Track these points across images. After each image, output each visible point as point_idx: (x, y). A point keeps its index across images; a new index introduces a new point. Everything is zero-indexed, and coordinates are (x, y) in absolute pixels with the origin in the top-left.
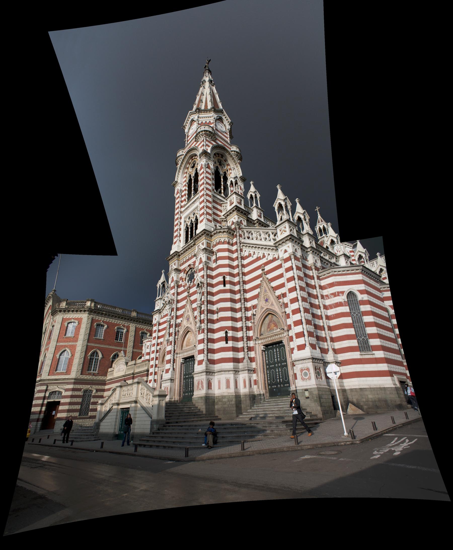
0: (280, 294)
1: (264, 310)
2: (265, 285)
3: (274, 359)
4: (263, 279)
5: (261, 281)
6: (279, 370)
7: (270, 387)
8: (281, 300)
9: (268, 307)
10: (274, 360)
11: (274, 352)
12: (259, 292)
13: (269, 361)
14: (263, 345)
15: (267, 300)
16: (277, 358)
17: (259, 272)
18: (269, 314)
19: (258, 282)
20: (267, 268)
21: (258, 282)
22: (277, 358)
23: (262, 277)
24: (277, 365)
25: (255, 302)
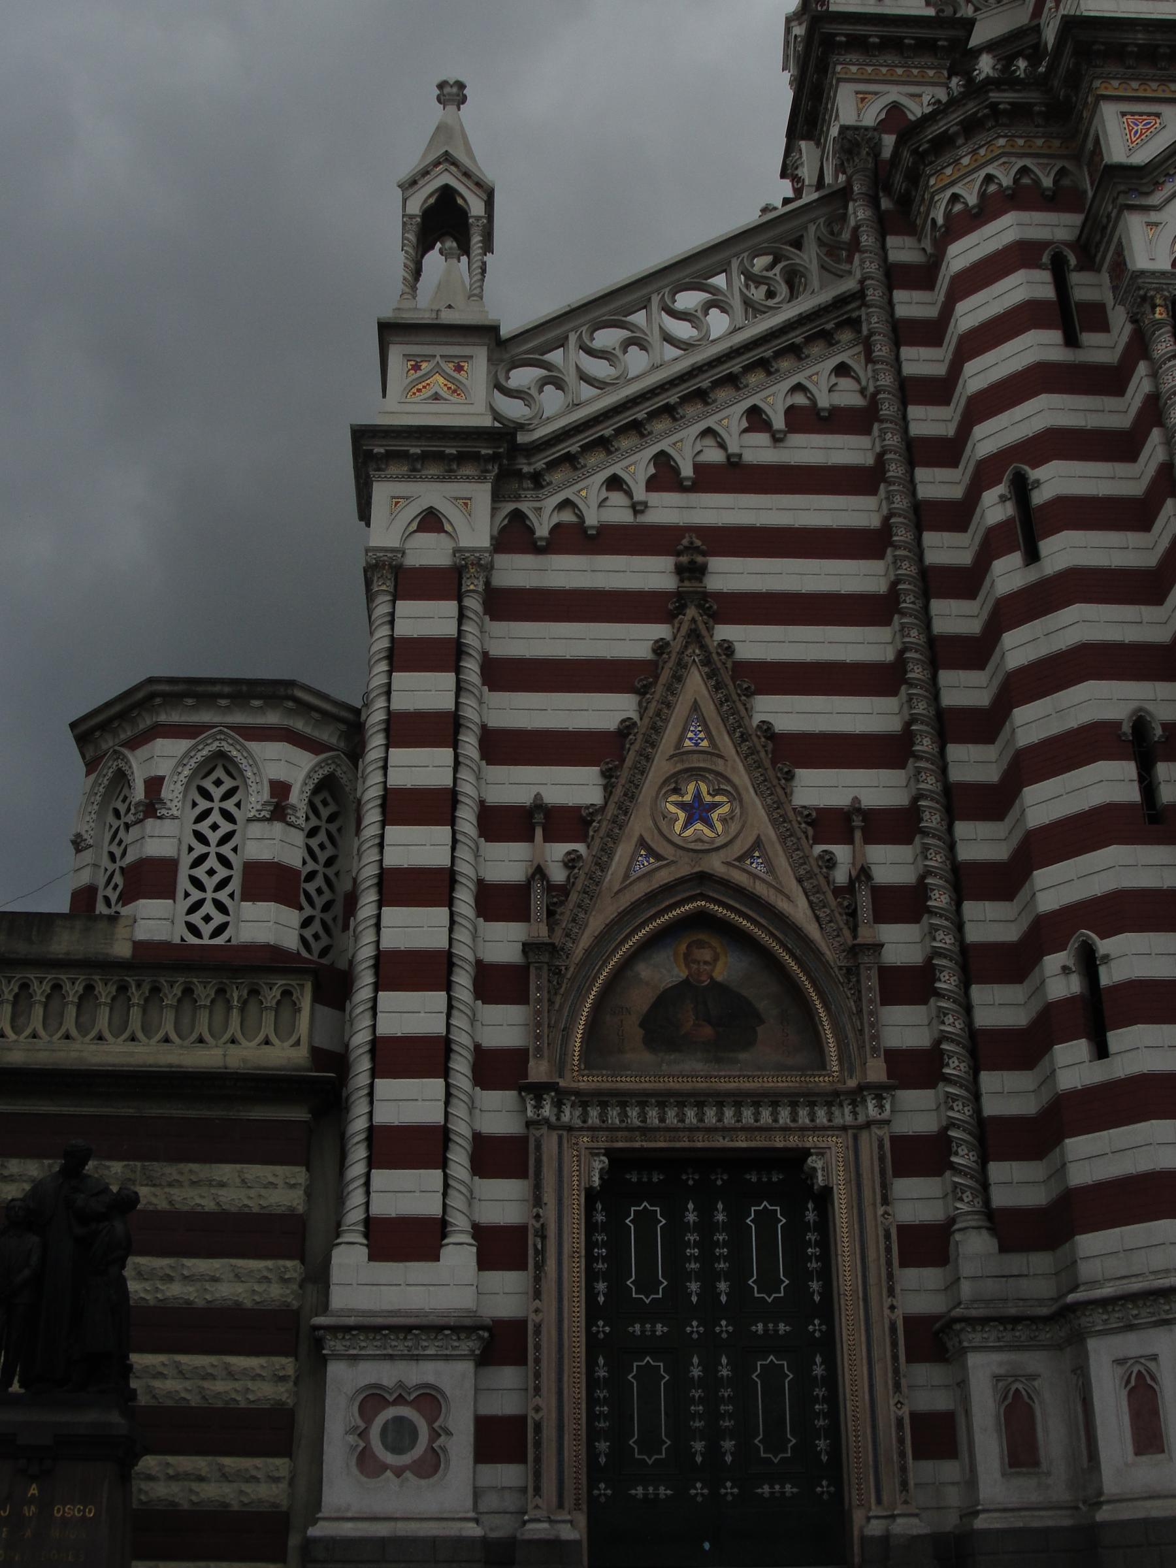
0: (840, 799)
1: (665, 877)
2: (695, 684)
3: (677, 1275)
4: (695, 636)
5: (660, 647)
6: (710, 1367)
7: (603, 1489)
8: (841, 852)
9: (716, 865)
10: (676, 1290)
11: (676, 1227)
12: (626, 729)
13: (617, 1290)
14: (608, 1152)
15: (698, 811)
16: (708, 1278)
17: (653, 573)
18: (701, 920)
19: (632, 641)
20: (730, 574)
21: (632, 641)
22: (708, 1278)
23: (668, 617)
24: (694, 1327)
25: (575, 786)
